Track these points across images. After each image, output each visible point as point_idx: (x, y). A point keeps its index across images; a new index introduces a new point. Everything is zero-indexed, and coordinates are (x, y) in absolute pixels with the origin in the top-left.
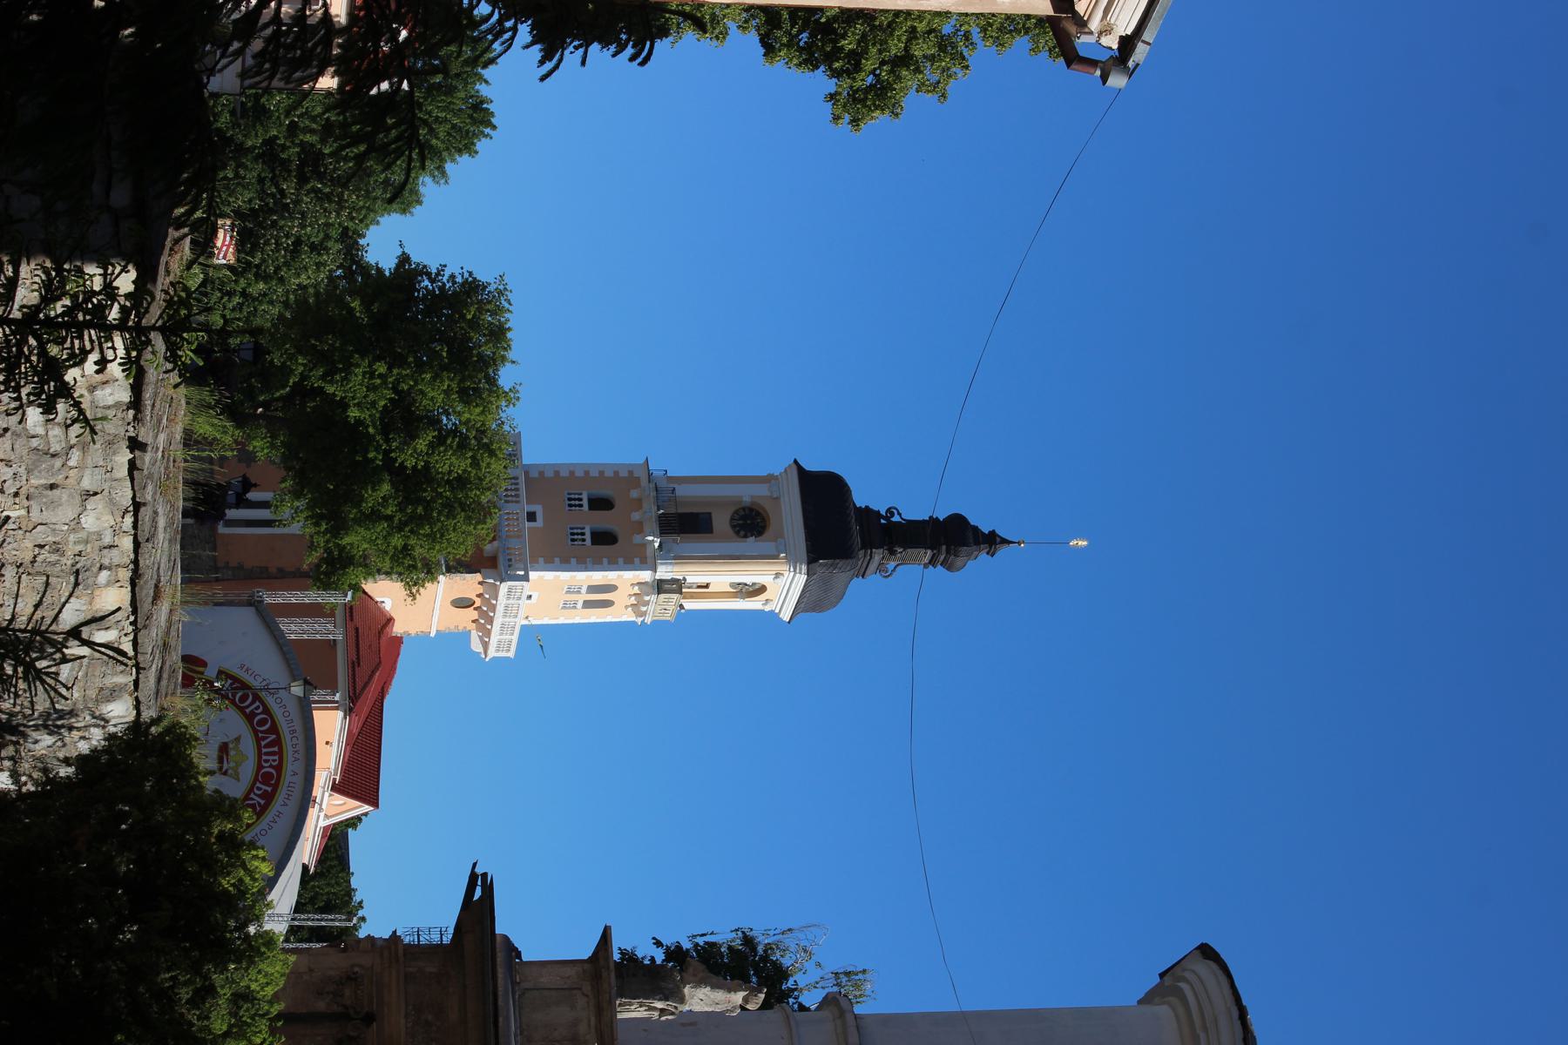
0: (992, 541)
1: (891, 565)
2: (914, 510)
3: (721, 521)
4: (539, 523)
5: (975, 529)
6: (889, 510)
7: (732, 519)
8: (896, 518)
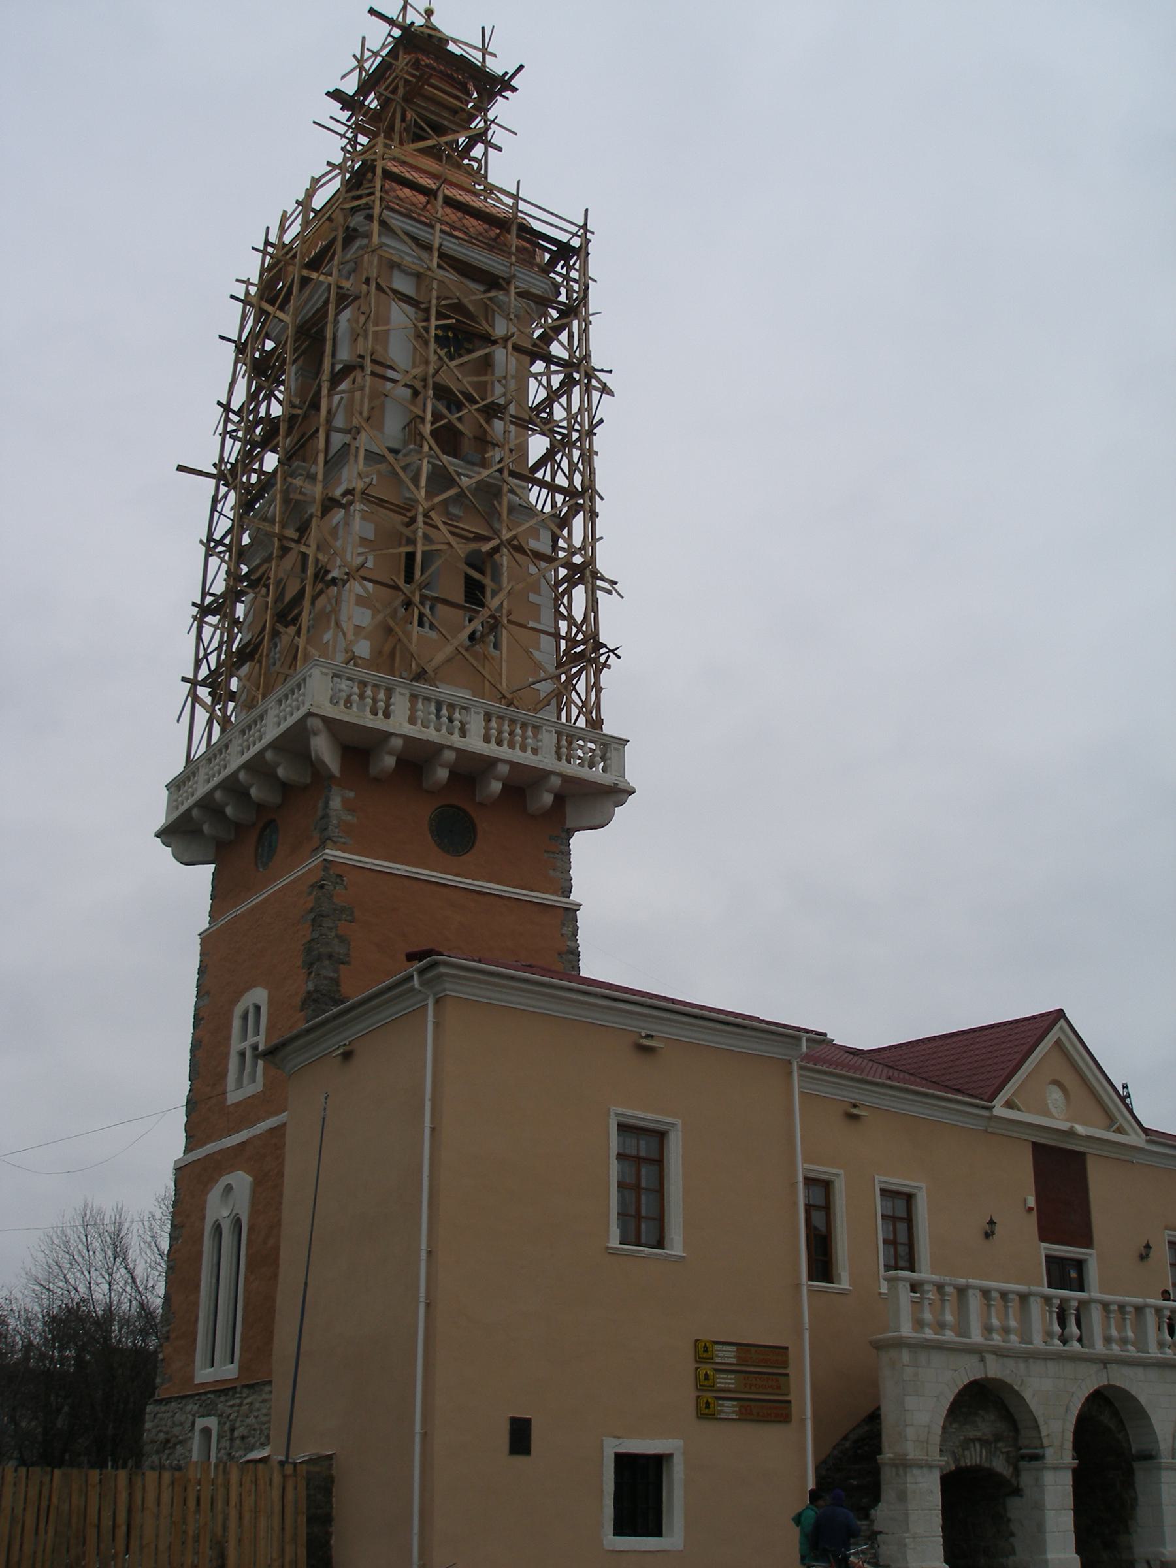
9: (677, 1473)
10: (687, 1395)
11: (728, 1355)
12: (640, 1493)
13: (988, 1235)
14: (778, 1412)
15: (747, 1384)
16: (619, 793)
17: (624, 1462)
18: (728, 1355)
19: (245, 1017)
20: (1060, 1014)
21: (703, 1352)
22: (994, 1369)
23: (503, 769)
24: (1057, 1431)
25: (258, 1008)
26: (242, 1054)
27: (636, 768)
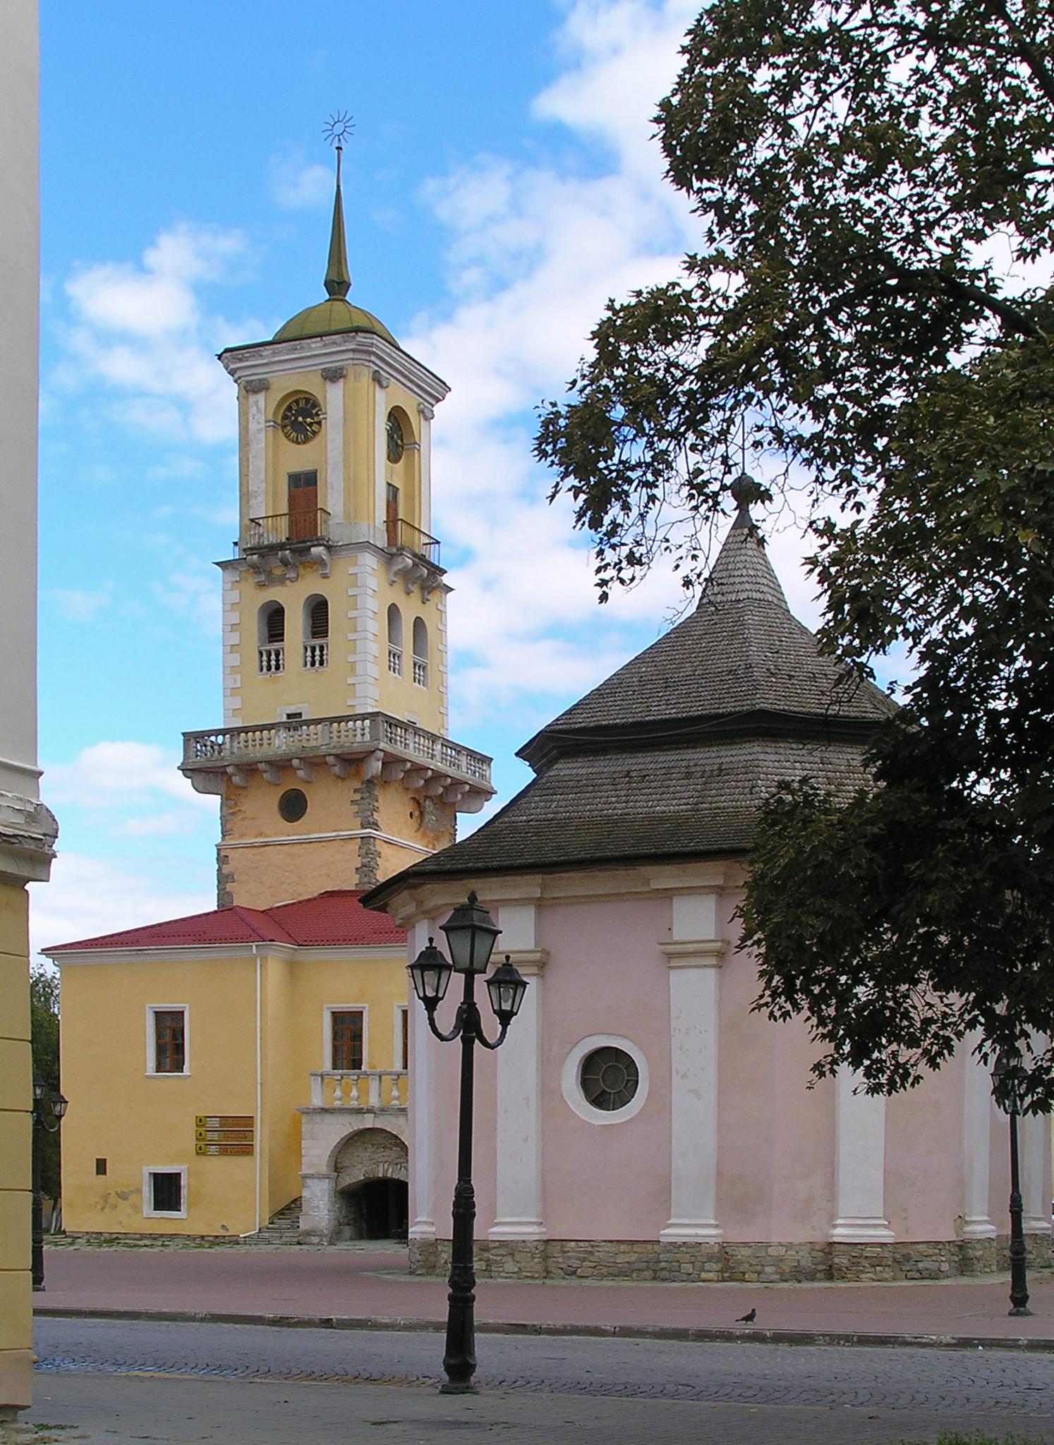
9: (183, 1182)
10: (190, 1143)
11: (215, 1123)
12: (167, 1191)
14: (247, 1150)
15: (231, 1136)
17: (158, 1178)
18: (215, 1123)
21: (200, 1121)
22: (369, 1122)
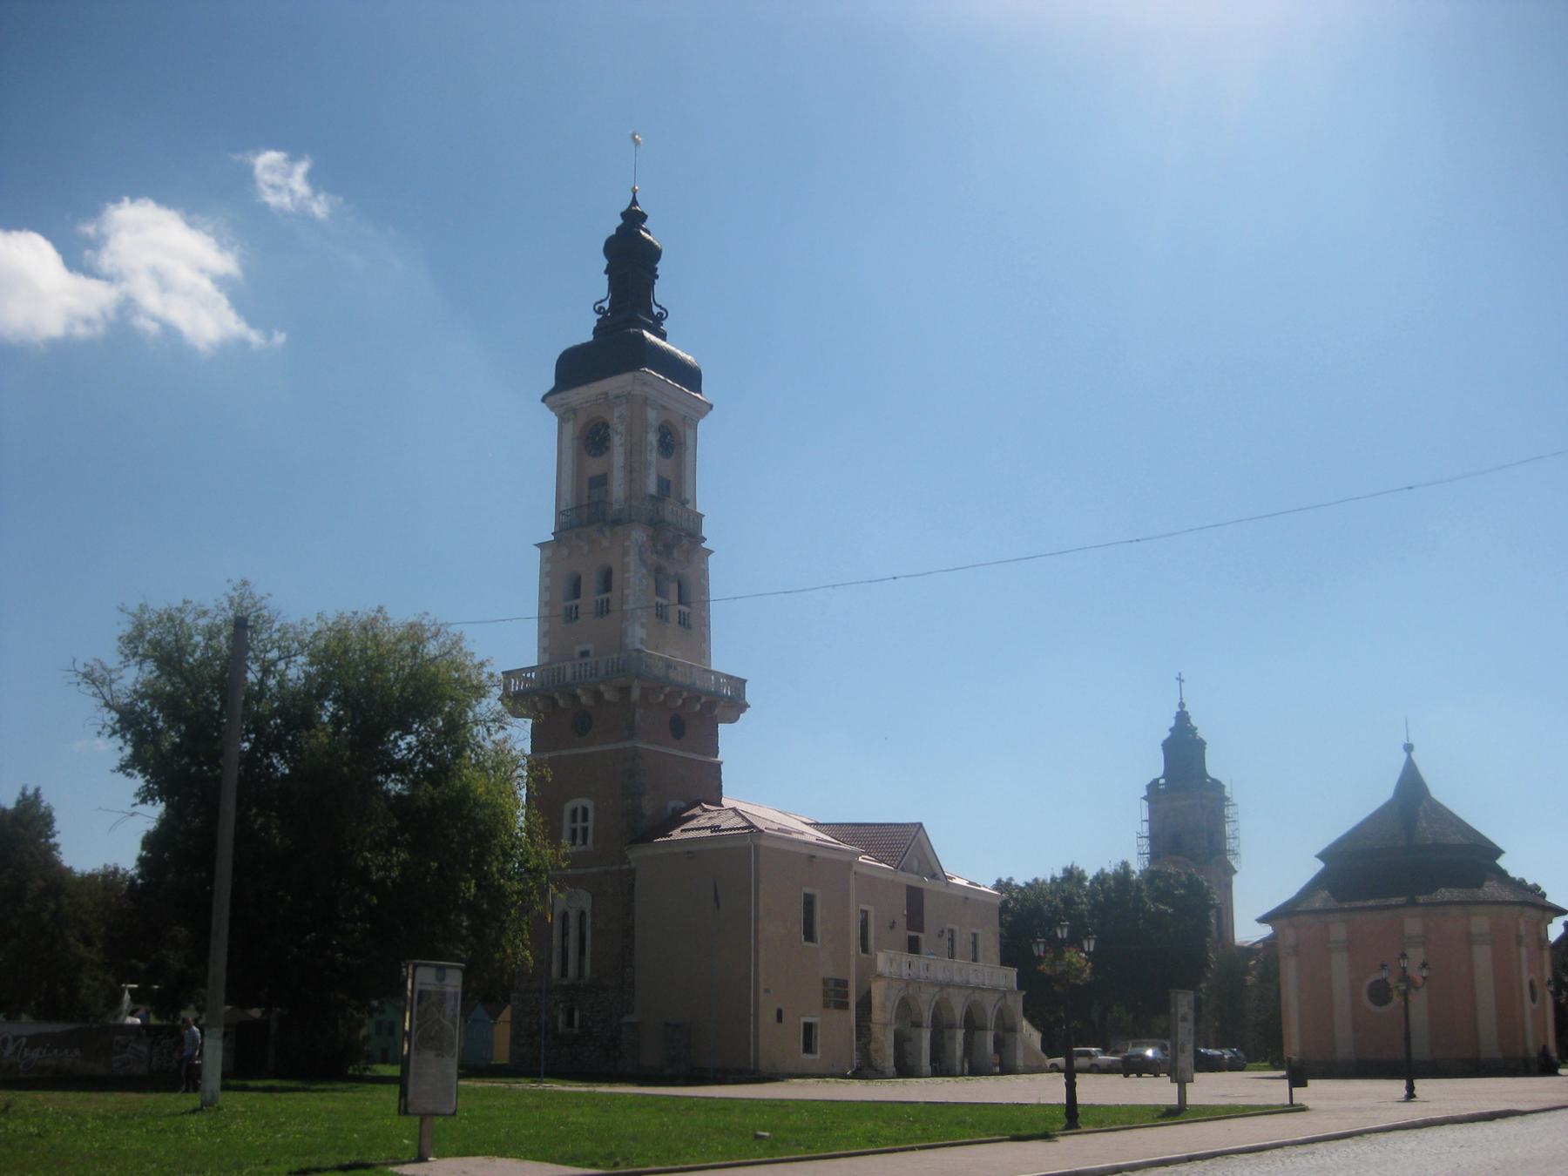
0: (633, 217)
1: (656, 310)
2: (599, 288)
3: (594, 466)
4: (589, 647)
5: (618, 229)
6: (598, 312)
7: (595, 455)
8: (606, 305)
13: (892, 928)
14: (843, 1006)
16: (743, 707)
19: (574, 812)
20: (921, 825)
21: (825, 981)
23: (704, 699)
24: (927, 1017)
25: (585, 810)
26: (574, 831)
27: (749, 697)
